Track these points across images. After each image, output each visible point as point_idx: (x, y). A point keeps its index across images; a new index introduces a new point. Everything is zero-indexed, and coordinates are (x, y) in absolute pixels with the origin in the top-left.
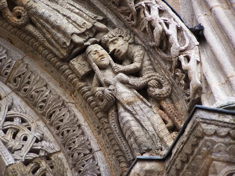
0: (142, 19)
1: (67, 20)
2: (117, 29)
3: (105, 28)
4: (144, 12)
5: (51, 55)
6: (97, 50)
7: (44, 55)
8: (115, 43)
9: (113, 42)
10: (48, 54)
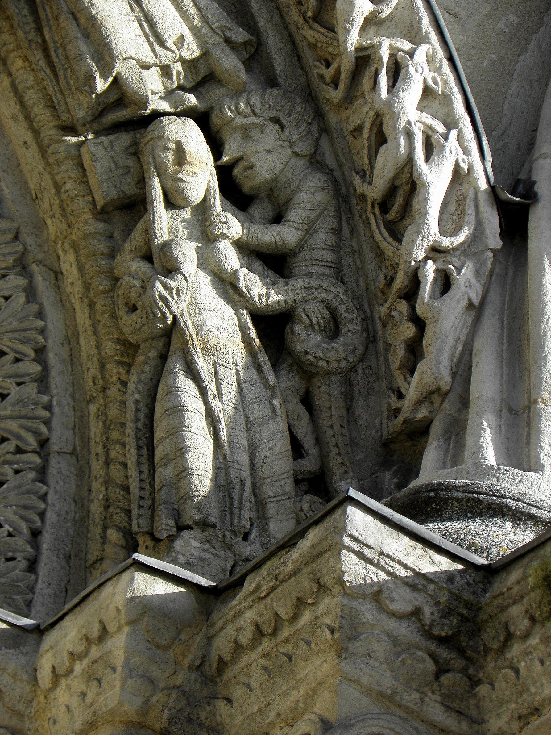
4: (377, 73)
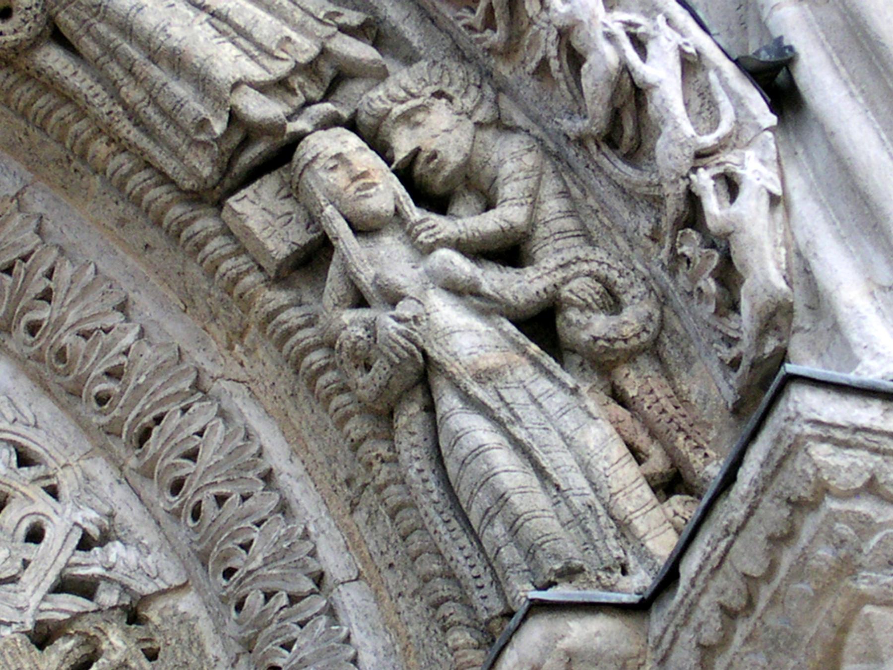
0: (531, 22)
1: (213, 26)
2: (423, 64)
3: (374, 62)
5: (144, 174)
6: (344, 151)
7: (113, 174)
8: (418, 124)
9: (406, 117)
10: (132, 172)
